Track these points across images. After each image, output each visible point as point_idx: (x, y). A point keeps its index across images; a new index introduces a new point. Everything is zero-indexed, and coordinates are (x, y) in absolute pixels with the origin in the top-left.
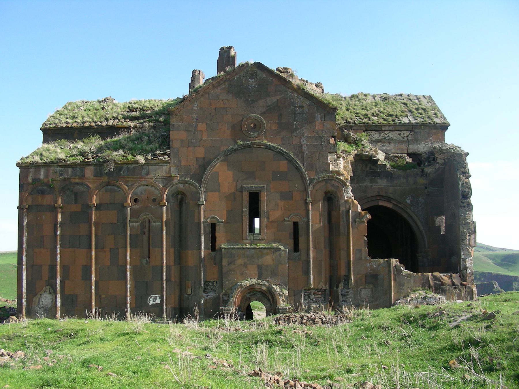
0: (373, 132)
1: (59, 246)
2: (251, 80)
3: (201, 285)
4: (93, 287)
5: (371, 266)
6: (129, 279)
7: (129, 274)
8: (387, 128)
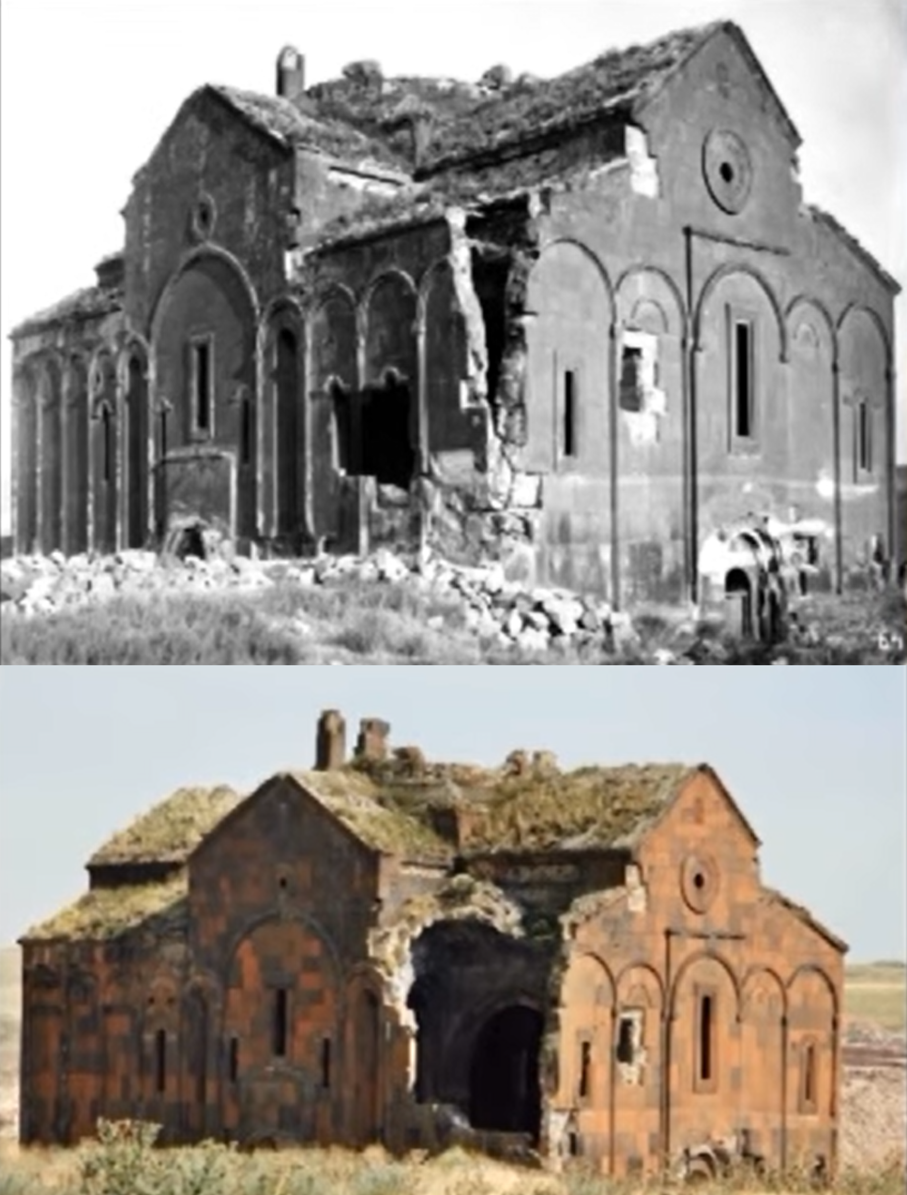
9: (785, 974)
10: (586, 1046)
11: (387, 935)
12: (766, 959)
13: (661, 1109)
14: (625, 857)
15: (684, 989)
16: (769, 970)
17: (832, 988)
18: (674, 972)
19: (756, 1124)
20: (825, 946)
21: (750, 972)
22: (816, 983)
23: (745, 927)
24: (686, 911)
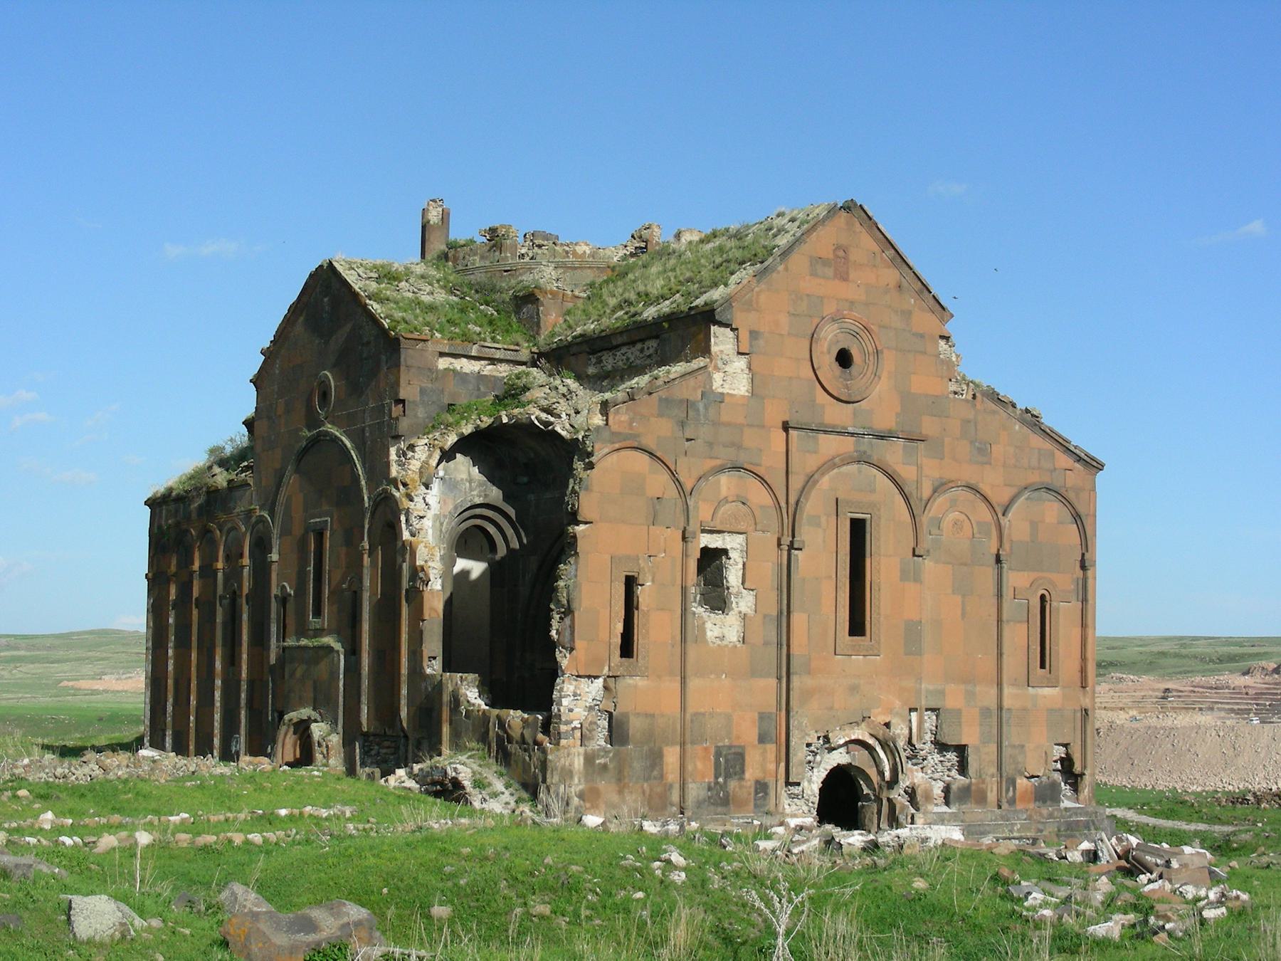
0: (605, 353)
1: (171, 645)
2: (326, 300)
3: (268, 717)
4: (192, 718)
5: (426, 688)
6: (218, 704)
7: (217, 695)
8: (620, 340)
9: (1000, 496)
10: (631, 583)
11: (412, 447)
12: (968, 473)
13: (779, 679)
14: (708, 317)
15: (815, 505)
16: (970, 487)
17: (1077, 518)
18: (796, 482)
19: (953, 699)
20: (1064, 460)
21: (940, 487)
22: (1052, 511)
23: (928, 426)
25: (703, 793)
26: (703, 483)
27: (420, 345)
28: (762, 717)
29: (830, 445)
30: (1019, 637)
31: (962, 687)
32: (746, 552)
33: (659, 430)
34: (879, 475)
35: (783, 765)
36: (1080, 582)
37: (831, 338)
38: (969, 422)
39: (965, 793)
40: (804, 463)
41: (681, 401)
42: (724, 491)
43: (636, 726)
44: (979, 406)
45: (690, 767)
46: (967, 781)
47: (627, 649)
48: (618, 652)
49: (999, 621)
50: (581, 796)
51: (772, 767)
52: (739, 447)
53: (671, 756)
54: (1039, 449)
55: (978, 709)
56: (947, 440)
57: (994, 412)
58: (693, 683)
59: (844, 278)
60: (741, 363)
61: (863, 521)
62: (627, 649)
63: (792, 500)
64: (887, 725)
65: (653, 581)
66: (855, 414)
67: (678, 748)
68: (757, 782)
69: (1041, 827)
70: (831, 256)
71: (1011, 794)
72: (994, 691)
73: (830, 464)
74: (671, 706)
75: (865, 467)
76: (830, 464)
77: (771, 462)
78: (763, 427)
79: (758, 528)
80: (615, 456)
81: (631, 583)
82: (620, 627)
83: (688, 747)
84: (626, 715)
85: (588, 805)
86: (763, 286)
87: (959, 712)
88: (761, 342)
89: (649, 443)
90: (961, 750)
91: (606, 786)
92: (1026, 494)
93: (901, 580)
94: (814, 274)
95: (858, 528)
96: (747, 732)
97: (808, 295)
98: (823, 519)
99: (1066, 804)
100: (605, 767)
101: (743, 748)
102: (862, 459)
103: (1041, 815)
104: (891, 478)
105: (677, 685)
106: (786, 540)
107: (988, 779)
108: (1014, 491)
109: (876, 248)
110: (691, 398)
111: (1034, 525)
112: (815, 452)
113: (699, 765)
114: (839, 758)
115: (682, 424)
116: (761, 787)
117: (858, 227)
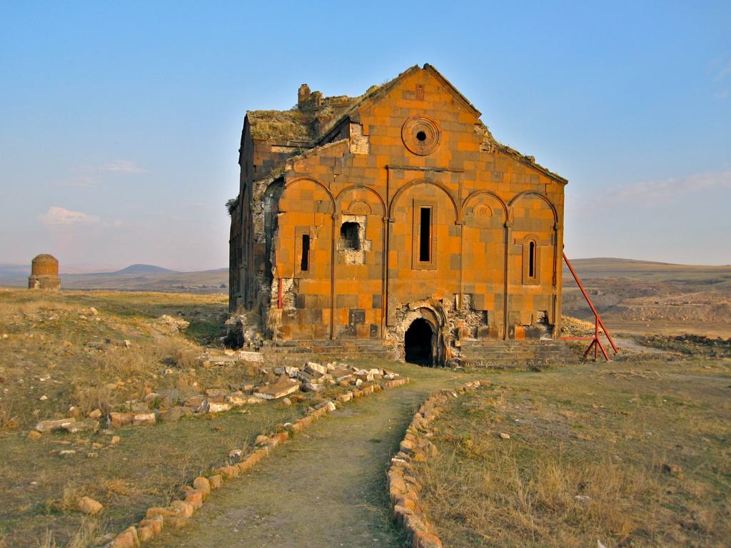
8: (333, 135)
10: (306, 239)
13: (383, 280)
15: (399, 203)
17: (552, 206)
18: (392, 193)
20: (545, 180)
22: (538, 203)
23: (468, 165)
24: (407, 154)
25: (343, 330)
26: (343, 194)
27: (263, 142)
28: (374, 297)
29: (410, 175)
30: (517, 263)
31: (485, 284)
32: (366, 224)
33: (321, 171)
34: (437, 189)
35: (384, 318)
36: (554, 236)
37: (414, 127)
38: (491, 163)
39: (486, 333)
40: (396, 183)
41: (332, 158)
42: (355, 197)
43: (309, 300)
44: (496, 156)
45: (335, 318)
46: (487, 327)
47: (305, 266)
48: (300, 268)
49: (506, 254)
50: (280, 329)
51: (380, 319)
52: (363, 177)
53: (326, 313)
54: (531, 175)
55: (493, 295)
56: (478, 172)
57: (505, 158)
58: (337, 282)
59: (422, 100)
60: (365, 140)
61: (428, 210)
62: (305, 266)
63: (390, 201)
64: (441, 301)
65: (318, 237)
66: (426, 162)
67: (329, 310)
68: (372, 325)
69: (526, 349)
70: (414, 90)
71: (512, 333)
72: (503, 286)
73: (410, 184)
74: (326, 292)
75: (429, 185)
76: (410, 184)
77: (380, 182)
78: (376, 168)
79: (373, 213)
80: (297, 183)
81: (306, 239)
82: (300, 257)
83: (335, 309)
84: (303, 295)
85: (284, 334)
86: (376, 105)
87: (483, 295)
88: (375, 130)
89: (316, 177)
90: (485, 312)
91: (293, 326)
92: (522, 196)
93: (449, 235)
94: (405, 98)
95: (426, 214)
96: (366, 303)
97: (401, 108)
98: (406, 209)
99: (543, 338)
100: (293, 318)
101: (365, 310)
102: (428, 181)
103: (528, 343)
104: (443, 189)
105: (330, 282)
106: (386, 218)
107: (499, 326)
108: (514, 195)
109: (439, 85)
110: (337, 156)
111: (527, 210)
112: (403, 179)
113: (341, 317)
114: (417, 315)
115: (333, 168)
116: (374, 327)
117: (430, 76)
